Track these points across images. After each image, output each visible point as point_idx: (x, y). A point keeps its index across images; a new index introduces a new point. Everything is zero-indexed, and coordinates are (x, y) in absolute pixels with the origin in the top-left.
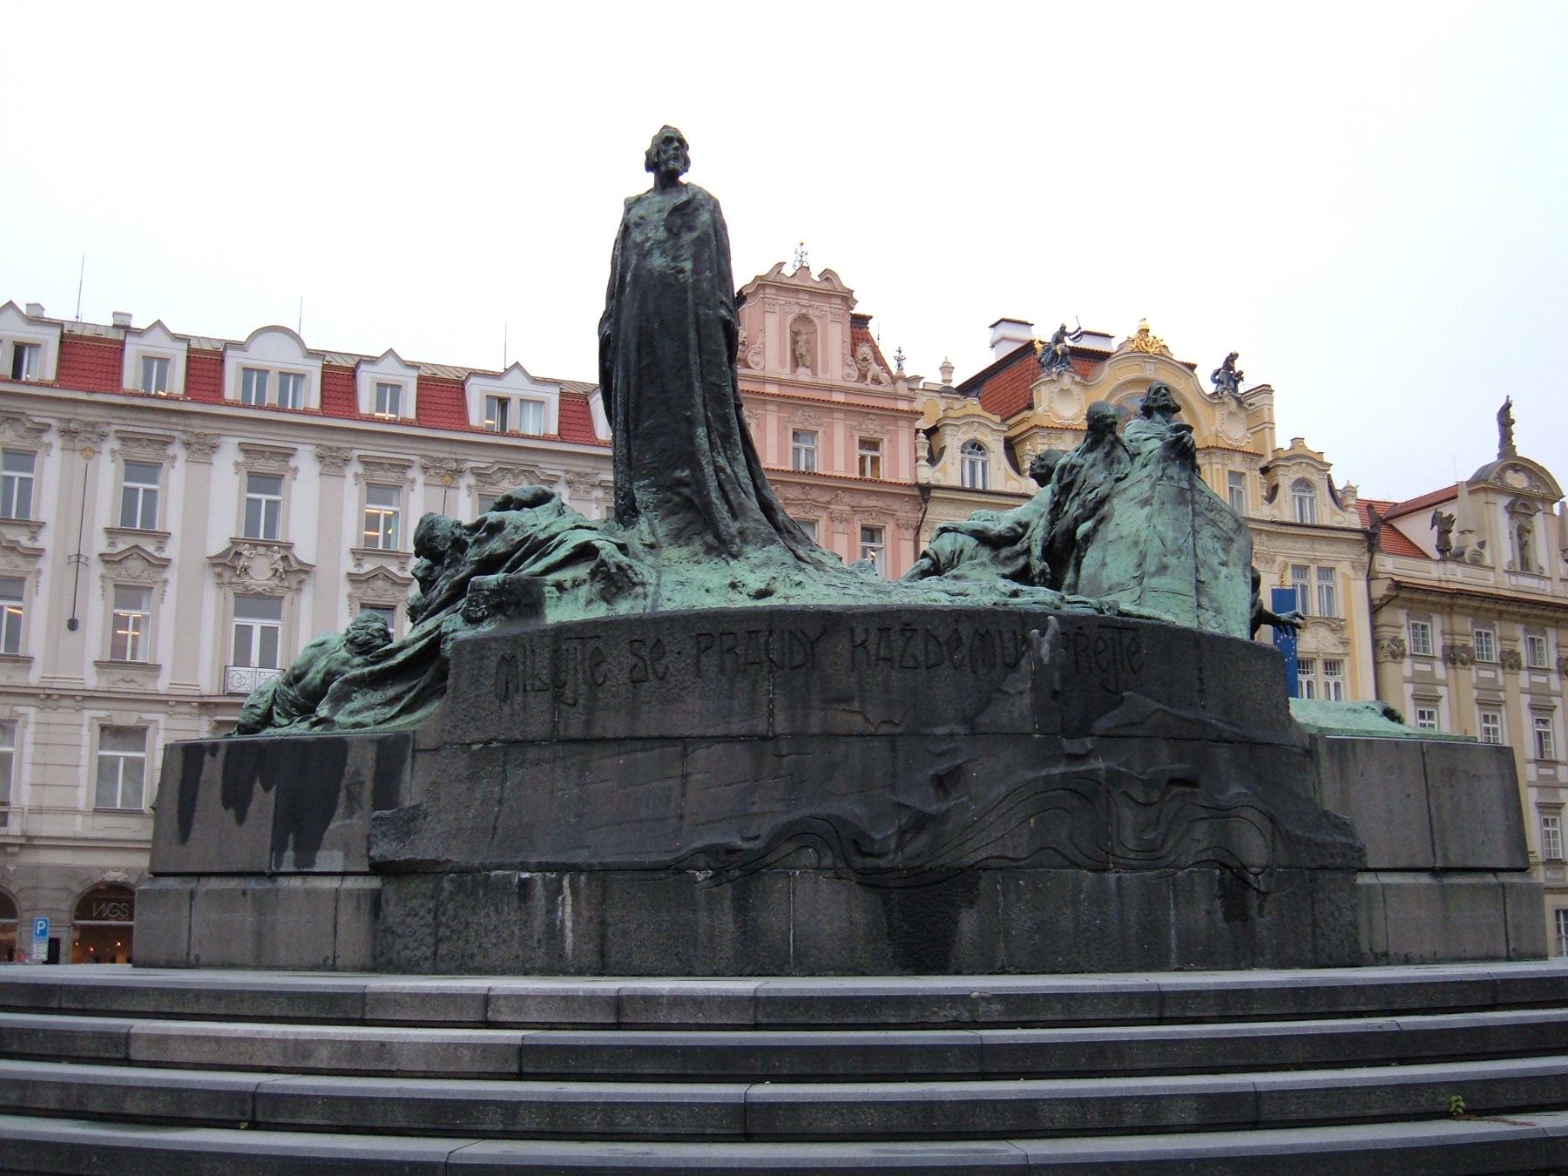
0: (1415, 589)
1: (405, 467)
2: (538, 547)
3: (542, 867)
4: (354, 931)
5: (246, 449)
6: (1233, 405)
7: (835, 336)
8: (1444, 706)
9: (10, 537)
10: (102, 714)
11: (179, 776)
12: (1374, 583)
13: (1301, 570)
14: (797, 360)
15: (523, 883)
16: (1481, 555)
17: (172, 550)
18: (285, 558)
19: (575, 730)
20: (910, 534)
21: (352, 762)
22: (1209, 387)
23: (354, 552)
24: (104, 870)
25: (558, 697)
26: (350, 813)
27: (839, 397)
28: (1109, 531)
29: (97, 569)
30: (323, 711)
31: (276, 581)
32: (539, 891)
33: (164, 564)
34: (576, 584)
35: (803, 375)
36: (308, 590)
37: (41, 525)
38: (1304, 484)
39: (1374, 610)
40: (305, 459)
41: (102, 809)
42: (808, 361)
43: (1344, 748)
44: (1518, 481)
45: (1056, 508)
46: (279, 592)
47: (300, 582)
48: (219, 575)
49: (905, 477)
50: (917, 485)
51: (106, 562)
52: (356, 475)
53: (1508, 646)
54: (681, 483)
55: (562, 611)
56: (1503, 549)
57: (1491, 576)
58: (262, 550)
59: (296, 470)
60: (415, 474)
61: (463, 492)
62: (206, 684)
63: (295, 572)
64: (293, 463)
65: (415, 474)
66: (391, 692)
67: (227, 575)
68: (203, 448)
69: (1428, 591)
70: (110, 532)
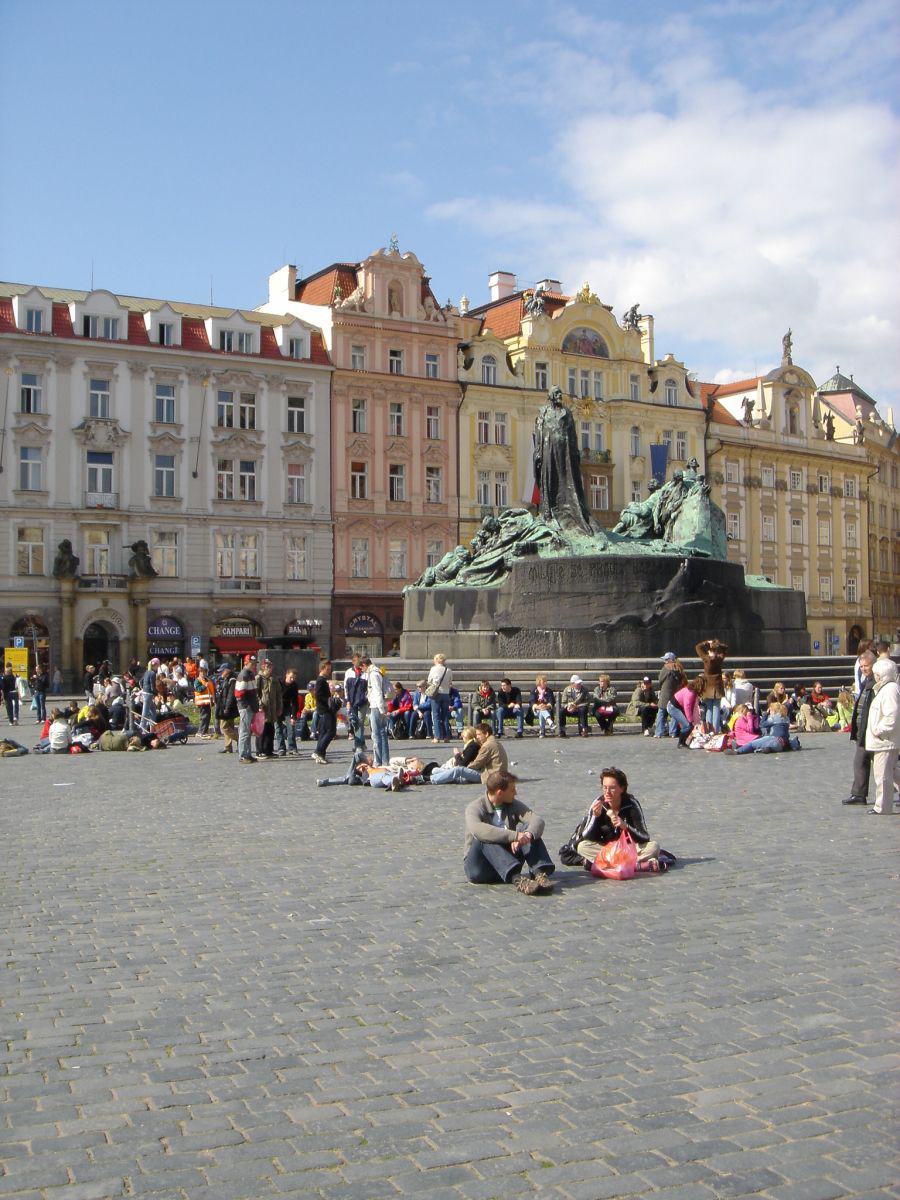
0: (731, 444)
1: (176, 374)
2: (531, 531)
4: (485, 646)
6: (636, 333)
7: (413, 292)
8: (743, 512)
10: (20, 520)
11: (417, 600)
12: (709, 441)
13: (668, 433)
14: (391, 309)
16: (769, 425)
18: (115, 429)
19: (556, 590)
20: (453, 411)
21: (479, 597)
22: (621, 323)
24: (27, 608)
26: (480, 612)
27: (415, 329)
28: (683, 517)
29: (11, 436)
30: (460, 579)
32: (552, 638)
35: (396, 316)
38: (671, 382)
39: (708, 457)
40: (122, 371)
41: (23, 574)
42: (398, 308)
44: (792, 379)
45: (662, 505)
49: (451, 377)
50: (458, 382)
51: (16, 433)
53: (780, 477)
54: (566, 509)
56: (782, 421)
57: (773, 436)
59: (117, 376)
60: (183, 377)
61: (210, 388)
62: (75, 500)
63: (119, 436)
64: (115, 372)
65: (183, 377)
66: (485, 575)
68: (65, 364)
69: (740, 446)
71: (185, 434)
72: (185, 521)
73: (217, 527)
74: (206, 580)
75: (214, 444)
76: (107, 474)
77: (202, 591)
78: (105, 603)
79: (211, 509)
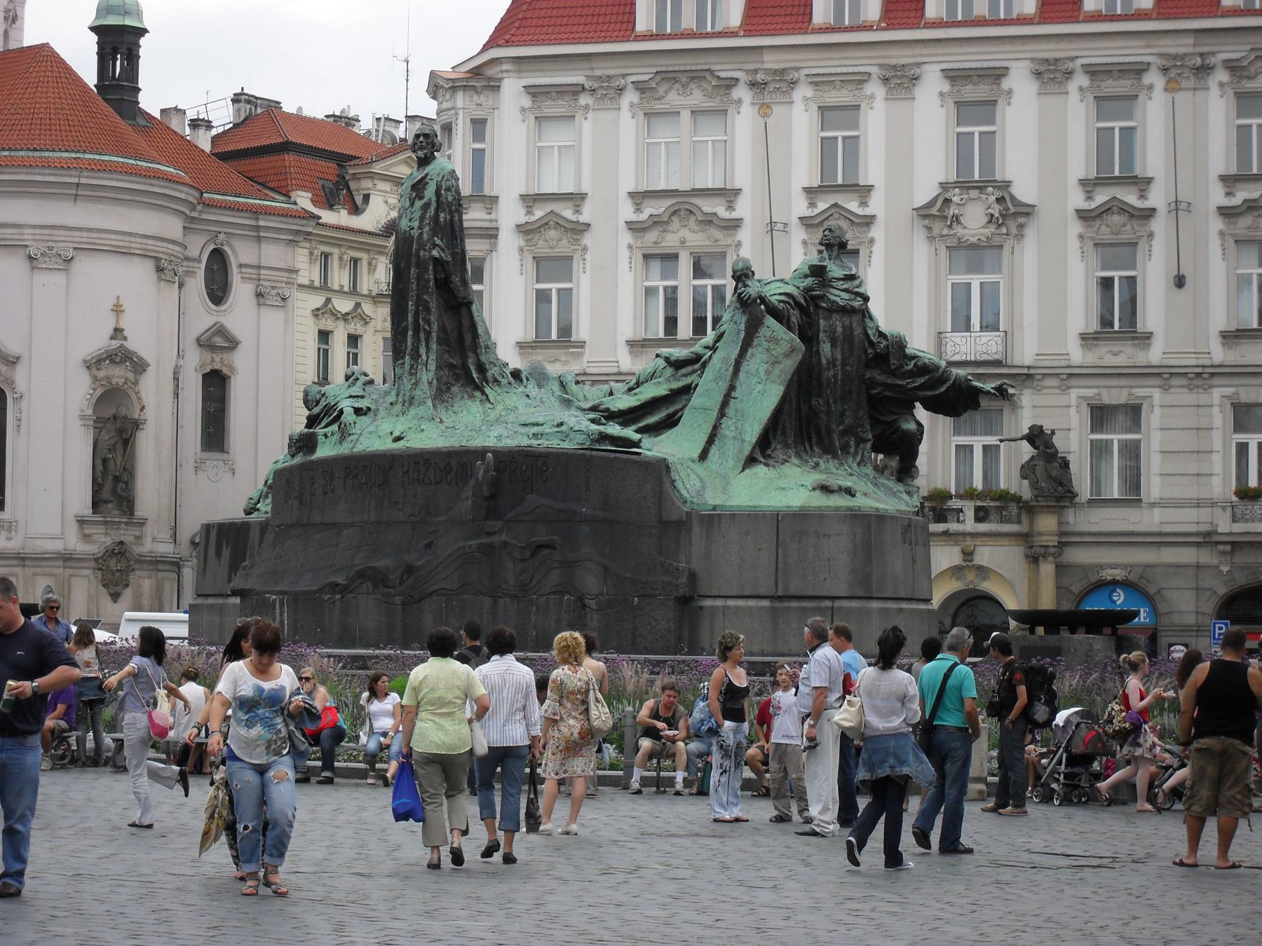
1: (1138, 70)
3: (277, 593)
5: (953, 76)
9: (707, 209)
15: (274, 601)
17: (876, 205)
18: (1000, 200)
23: (1083, 183)
25: (301, 502)
31: (992, 228)
33: (869, 221)
34: (333, 434)
36: (1031, 234)
37: (737, 192)
40: (1020, 82)
43: (714, 520)
46: (997, 240)
47: (1021, 226)
48: (929, 228)
52: (1081, 89)
55: (324, 451)
58: (974, 194)
59: (1010, 92)
60: (1154, 78)
61: (1214, 90)
63: (1012, 214)
64: (1006, 84)
65: (1154, 78)
67: (938, 227)
68: (901, 81)
70: (809, 191)
71: (1157, 198)
72: (1157, 381)
73: (1229, 391)
74: (1198, 504)
75: (1227, 213)
76: (990, 293)
77: (1194, 529)
78: (968, 555)
79: (1219, 354)
